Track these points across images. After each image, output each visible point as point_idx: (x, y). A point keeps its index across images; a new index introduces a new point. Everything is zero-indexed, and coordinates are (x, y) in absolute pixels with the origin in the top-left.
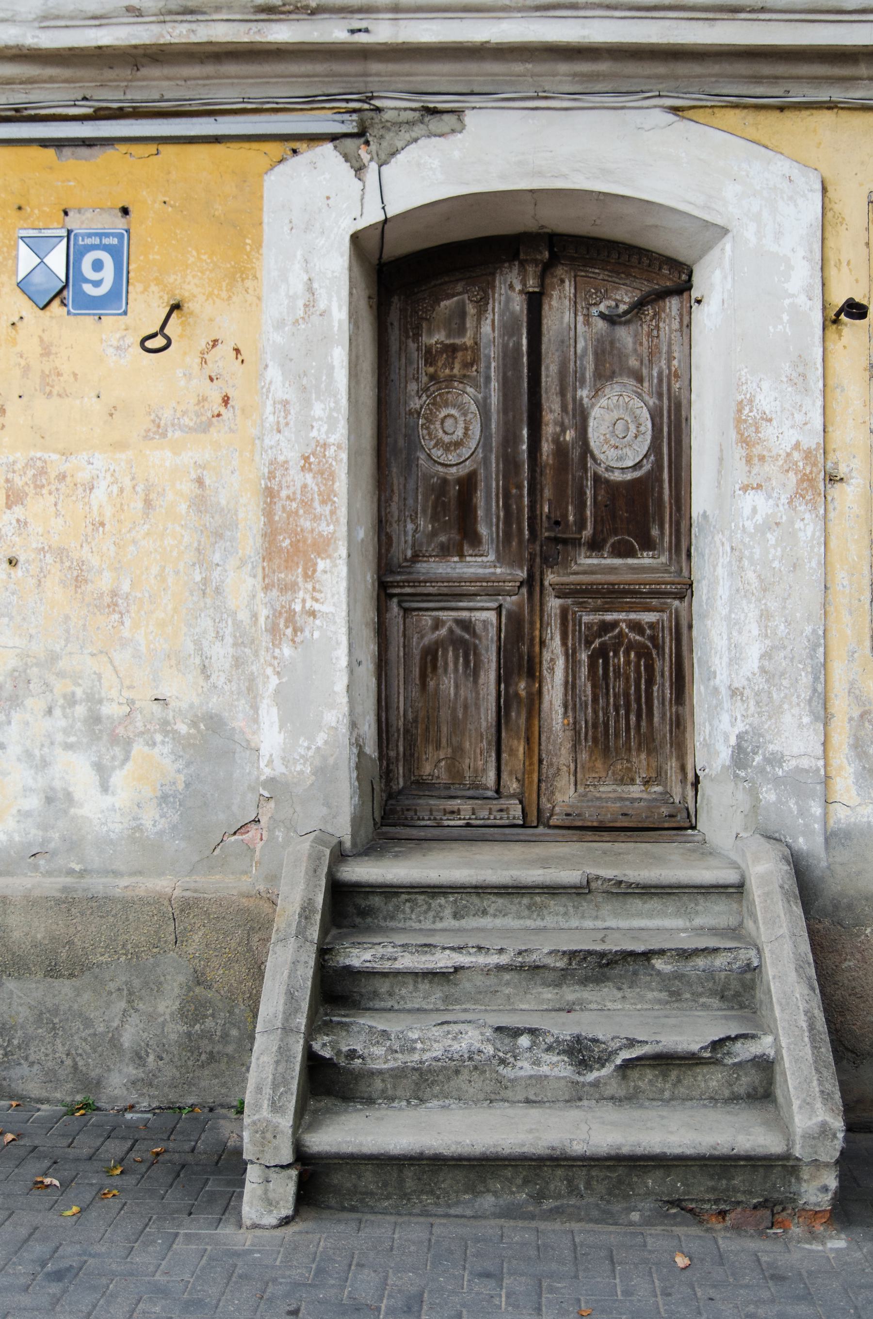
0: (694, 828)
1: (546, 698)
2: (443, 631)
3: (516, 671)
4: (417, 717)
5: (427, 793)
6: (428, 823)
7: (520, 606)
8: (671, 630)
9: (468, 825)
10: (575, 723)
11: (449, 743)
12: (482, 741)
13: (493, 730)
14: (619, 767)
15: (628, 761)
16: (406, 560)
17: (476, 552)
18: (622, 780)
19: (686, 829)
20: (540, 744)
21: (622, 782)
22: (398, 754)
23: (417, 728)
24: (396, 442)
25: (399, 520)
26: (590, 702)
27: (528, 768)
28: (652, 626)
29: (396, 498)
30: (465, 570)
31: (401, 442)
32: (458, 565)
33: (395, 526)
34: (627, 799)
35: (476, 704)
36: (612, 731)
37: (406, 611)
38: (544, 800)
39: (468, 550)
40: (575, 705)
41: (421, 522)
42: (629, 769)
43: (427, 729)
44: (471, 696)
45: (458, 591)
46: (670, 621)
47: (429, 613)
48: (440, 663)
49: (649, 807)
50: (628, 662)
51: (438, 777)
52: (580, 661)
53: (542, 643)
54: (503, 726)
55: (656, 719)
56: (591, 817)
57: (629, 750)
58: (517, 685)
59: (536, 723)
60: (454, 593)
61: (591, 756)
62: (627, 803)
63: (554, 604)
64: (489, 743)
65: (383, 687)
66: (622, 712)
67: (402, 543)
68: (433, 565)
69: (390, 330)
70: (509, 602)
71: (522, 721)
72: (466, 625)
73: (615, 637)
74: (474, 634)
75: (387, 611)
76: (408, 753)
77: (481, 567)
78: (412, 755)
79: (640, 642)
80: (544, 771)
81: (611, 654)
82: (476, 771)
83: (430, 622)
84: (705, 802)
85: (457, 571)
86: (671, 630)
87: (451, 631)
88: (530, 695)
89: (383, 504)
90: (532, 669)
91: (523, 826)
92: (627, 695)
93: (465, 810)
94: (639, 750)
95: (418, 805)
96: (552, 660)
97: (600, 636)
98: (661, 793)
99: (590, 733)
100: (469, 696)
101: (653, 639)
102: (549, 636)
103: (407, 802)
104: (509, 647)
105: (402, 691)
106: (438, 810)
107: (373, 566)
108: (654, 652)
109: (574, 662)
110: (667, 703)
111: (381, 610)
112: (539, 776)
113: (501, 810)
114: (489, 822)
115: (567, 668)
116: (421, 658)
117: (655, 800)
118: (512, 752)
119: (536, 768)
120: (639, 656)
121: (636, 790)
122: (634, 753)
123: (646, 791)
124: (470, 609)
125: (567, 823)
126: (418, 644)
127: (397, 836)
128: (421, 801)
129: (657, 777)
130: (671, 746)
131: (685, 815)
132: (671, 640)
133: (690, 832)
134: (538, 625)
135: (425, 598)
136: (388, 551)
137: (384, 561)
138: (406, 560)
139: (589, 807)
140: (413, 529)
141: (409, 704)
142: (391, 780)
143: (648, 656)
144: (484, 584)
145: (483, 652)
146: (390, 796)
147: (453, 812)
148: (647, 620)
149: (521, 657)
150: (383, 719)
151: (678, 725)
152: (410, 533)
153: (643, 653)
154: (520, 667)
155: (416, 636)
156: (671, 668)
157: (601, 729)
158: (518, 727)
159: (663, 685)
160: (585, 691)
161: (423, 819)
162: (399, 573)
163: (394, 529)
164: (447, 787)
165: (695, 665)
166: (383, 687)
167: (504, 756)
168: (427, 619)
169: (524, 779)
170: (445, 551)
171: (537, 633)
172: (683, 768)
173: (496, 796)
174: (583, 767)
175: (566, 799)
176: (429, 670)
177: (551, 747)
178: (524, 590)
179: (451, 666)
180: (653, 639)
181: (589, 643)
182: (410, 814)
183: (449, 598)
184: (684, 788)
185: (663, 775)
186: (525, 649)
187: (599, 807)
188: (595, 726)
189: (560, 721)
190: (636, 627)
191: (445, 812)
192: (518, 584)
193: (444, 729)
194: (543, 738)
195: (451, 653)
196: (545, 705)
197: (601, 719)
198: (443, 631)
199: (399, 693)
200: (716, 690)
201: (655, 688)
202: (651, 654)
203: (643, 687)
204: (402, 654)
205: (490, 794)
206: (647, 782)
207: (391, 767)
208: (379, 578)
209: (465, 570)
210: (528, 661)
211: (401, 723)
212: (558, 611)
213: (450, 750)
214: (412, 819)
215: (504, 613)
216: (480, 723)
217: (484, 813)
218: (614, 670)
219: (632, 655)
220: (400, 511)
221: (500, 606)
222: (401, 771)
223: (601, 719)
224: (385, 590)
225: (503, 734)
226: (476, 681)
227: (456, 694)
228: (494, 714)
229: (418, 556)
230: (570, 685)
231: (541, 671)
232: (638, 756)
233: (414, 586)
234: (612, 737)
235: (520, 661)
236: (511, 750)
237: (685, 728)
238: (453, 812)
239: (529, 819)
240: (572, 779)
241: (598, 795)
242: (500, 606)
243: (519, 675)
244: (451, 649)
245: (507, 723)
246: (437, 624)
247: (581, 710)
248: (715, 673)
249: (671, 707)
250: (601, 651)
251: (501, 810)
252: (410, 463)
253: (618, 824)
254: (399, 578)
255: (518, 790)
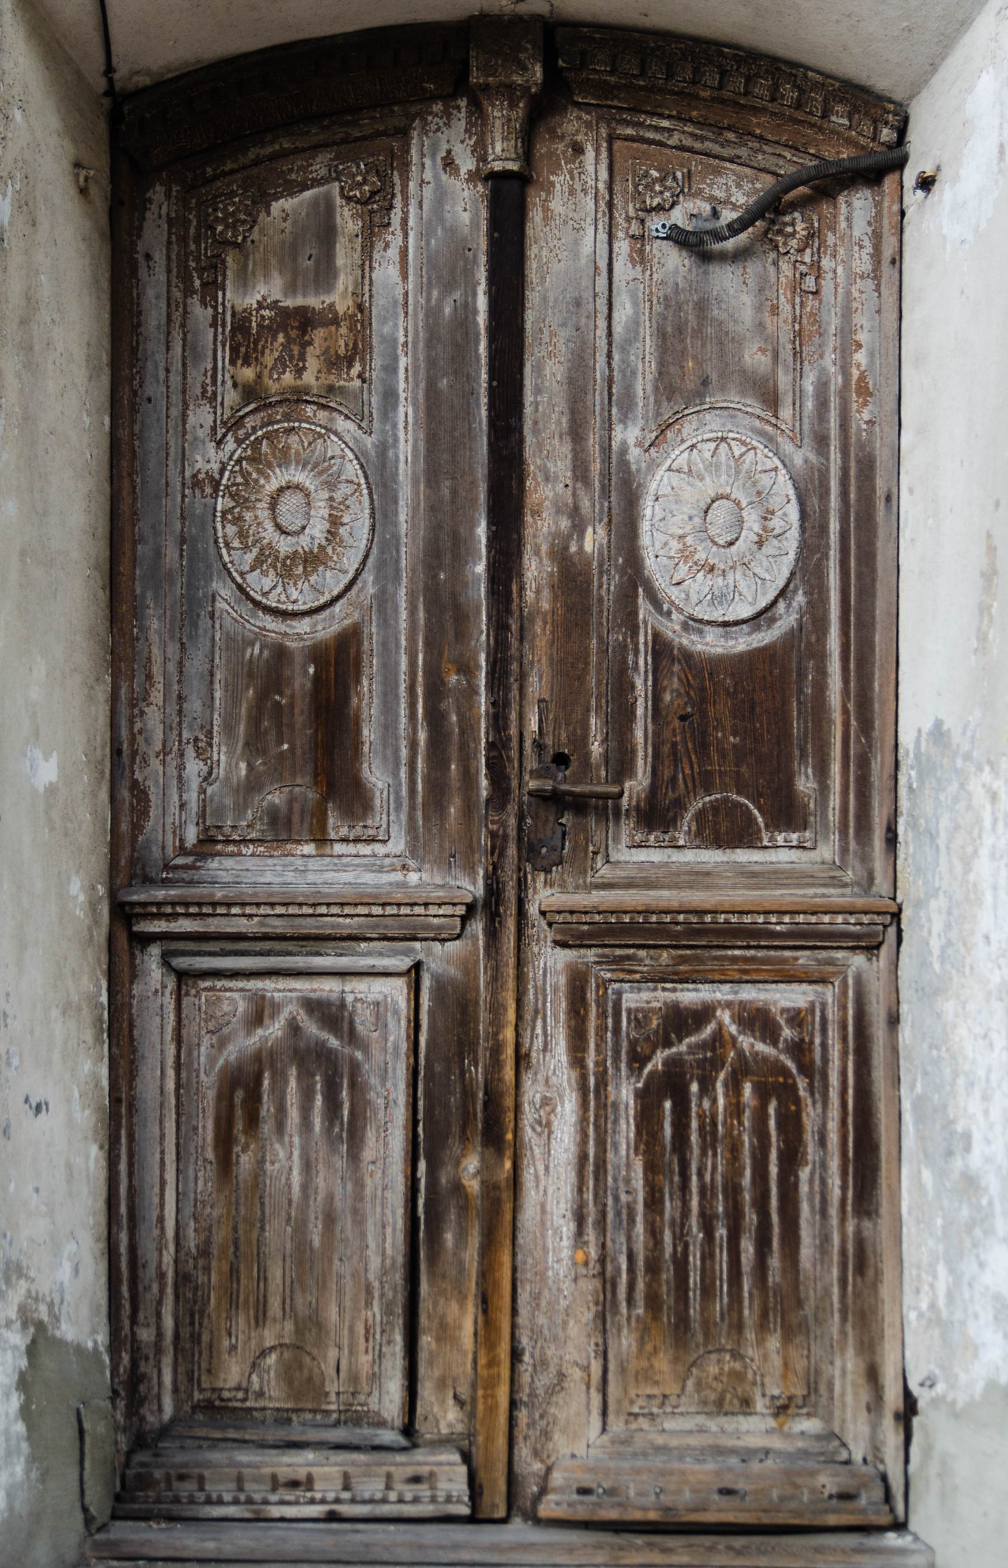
0: (900, 1526)
1: (531, 1197)
2: (274, 1030)
3: (455, 1129)
4: (208, 1242)
5: (231, 1434)
6: (232, 1511)
7: (468, 968)
8: (844, 1027)
9: (332, 1517)
10: (602, 1260)
11: (288, 1309)
12: (368, 1304)
13: (398, 1277)
14: (713, 1369)
15: (736, 1355)
16: (183, 851)
17: (358, 831)
18: (720, 1403)
19: (881, 1529)
20: (514, 1312)
21: (719, 1407)
22: (160, 1335)
23: (207, 1269)
24: (158, 554)
25: (165, 751)
26: (640, 1208)
27: (483, 1372)
28: (796, 1018)
29: (157, 696)
30: (329, 876)
31: (171, 555)
32: (313, 864)
33: (155, 764)
34: (733, 1451)
35: (355, 1211)
36: (694, 1279)
37: (183, 976)
38: (523, 1452)
39: (335, 825)
40: (603, 1214)
41: (221, 755)
42: (738, 1376)
43: (234, 1272)
44: (342, 1193)
45: (309, 926)
46: (844, 1007)
47: (240, 984)
48: (267, 1107)
49: (787, 1473)
50: (736, 1109)
51: (260, 1394)
52: (615, 1105)
53: (522, 1059)
54: (423, 1267)
55: (807, 1251)
56: (641, 1501)
57: (739, 1327)
58: (458, 1164)
59: (506, 1259)
60: (301, 934)
61: (641, 1342)
62: (734, 1461)
63: (551, 963)
64: (388, 1310)
65: (123, 1167)
66: (721, 1232)
67: (174, 809)
68: (250, 863)
69: (143, 272)
70: (441, 958)
71: (471, 1255)
72: (332, 1015)
73: (703, 1046)
74: (352, 1037)
75: (134, 976)
76: (185, 1332)
77: (370, 868)
78: (195, 1338)
79: (765, 1059)
80: (525, 1379)
81: (694, 1087)
82: (354, 1378)
83: (242, 1006)
84: (934, 1469)
85: (311, 877)
86: (844, 1027)
87: (294, 1028)
88: (490, 1188)
89: (124, 710)
90: (495, 1125)
91: (472, 1520)
92: (733, 1190)
93: (326, 1478)
94: (763, 1327)
95: (207, 1464)
96: (546, 1101)
97: (668, 1044)
98: (818, 1438)
99: (640, 1285)
100: (338, 1191)
101: (799, 1049)
102: (539, 1043)
103: (180, 1458)
104: (438, 1068)
105: (170, 1176)
106: (257, 1479)
107: (97, 862)
108: (802, 1083)
109: (602, 1105)
110: (833, 1211)
111: (119, 975)
112: (512, 1391)
113: (416, 1479)
114: (385, 1510)
115: (583, 1120)
116: (220, 1097)
117: (805, 1453)
118: (446, 1333)
119: (505, 1372)
120: (763, 1093)
121: (754, 1429)
122: (750, 1335)
123: (779, 1431)
124: (343, 974)
125: (581, 1513)
126: (212, 1060)
127: (147, 1551)
128: (216, 1456)
129: (808, 1396)
130: (844, 1319)
131: (878, 1494)
132: (844, 1054)
133: (892, 1539)
134: (511, 1015)
135: (229, 946)
136: (137, 827)
137: (126, 853)
138: (183, 851)
139: (637, 1472)
140: (201, 775)
141: (188, 1210)
142: (142, 1401)
143: (788, 1093)
144: (377, 910)
145: (374, 1080)
146: (140, 1441)
147: (294, 1484)
148: (785, 1004)
149: (467, 1094)
150: (123, 1249)
151: (861, 1267)
152: (195, 784)
153: (776, 1086)
154: (467, 1118)
155: (206, 1040)
156: (844, 1122)
157: (667, 1274)
158: (462, 1269)
159: (824, 1165)
160: (628, 1181)
161: (220, 1502)
162: (165, 883)
163: (153, 773)
164: (283, 1418)
165: (908, 1117)
166: (123, 1167)
167: (426, 1341)
168: (234, 1000)
169: (474, 1399)
170: (279, 830)
171: (509, 1034)
172: (873, 1375)
173: (403, 1442)
174: (623, 1370)
175: (580, 1450)
176: (239, 1125)
177: (542, 1320)
178: (477, 927)
179: (294, 1114)
180: (799, 1049)
181: (638, 1060)
182: (187, 1488)
183: (290, 946)
184: (875, 1426)
185: (823, 1389)
186: (478, 1074)
187: (663, 1473)
188: (653, 1267)
189: (566, 1253)
190: (758, 1021)
191: (275, 1483)
192: (461, 910)
193: (276, 1273)
194: (524, 1296)
195: (293, 1084)
196: (529, 1214)
197: (668, 1250)
198: (274, 1030)
199: (163, 1183)
200: (971, 1183)
201: (804, 1174)
202: (794, 1088)
203: (774, 1170)
204: (171, 1085)
205: (389, 1436)
206: (782, 1409)
207: (143, 1368)
208: (112, 893)
209: (329, 876)
210: (486, 1105)
211: (168, 1257)
212: (563, 980)
213: (289, 1326)
214: (192, 1501)
215: (426, 983)
216: (365, 1260)
217: (373, 1487)
218: (701, 1128)
219: (747, 1089)
220: (167, 728)
221: (417, 966)
222: (167, 1378)
223: (668, 1250)
224: (129, 926)
225: (424, 1287)
226: (354, 1156)
227: (305, 1187)
228: (400, 1237)
229: (215, 842)
230: (592, 1167)
231: (516, 1130)
232: (761, 1342)
233: (201, 915)
234: (694, 1296)
235: (465, 1105)
236: (443, 1326)
237: (878, 1274)
238: (294, 1484)
239: (486, 1499)
240: (596, 1399)
241: (660, 1440)
242: (417, 967)
243: (464, 1138)
244: (293, 1072)
245: (433, 1258)
246: (260, 1012)
247: (618, 1227)
248: (967, 1138)
249: (843, 1220)
250: (672, 1082)
251: (416, 1479)
252: (191, 612)
253: (710, 1517)
254: (160, 894)
255: (459, 1428)
